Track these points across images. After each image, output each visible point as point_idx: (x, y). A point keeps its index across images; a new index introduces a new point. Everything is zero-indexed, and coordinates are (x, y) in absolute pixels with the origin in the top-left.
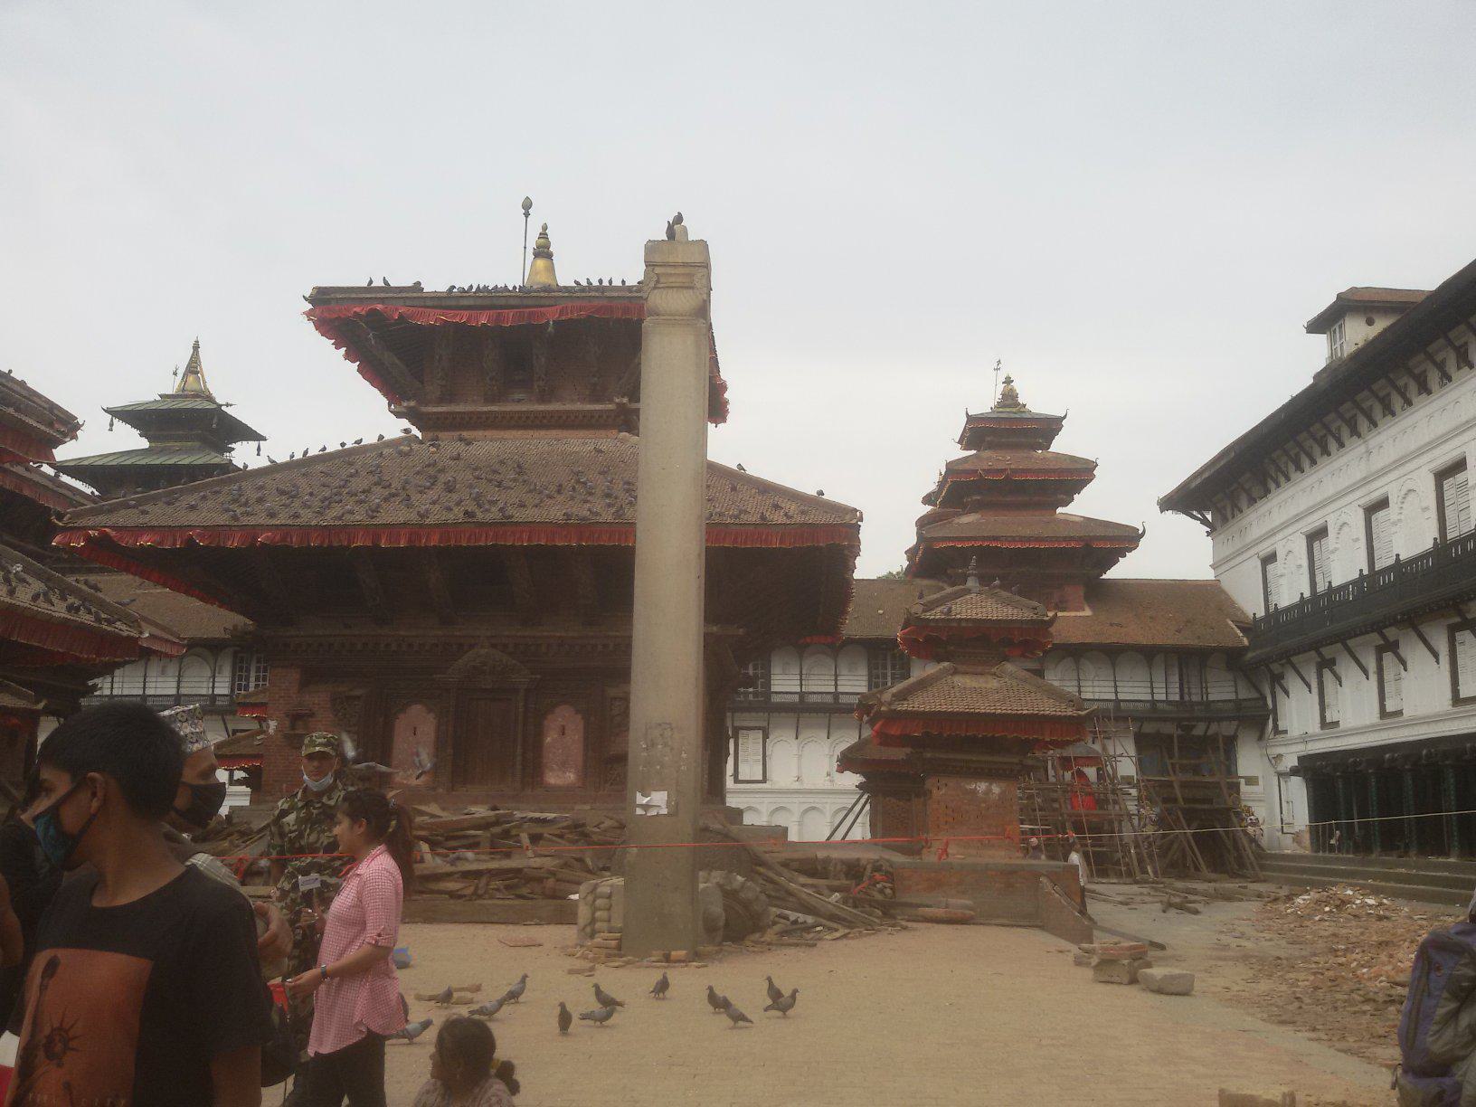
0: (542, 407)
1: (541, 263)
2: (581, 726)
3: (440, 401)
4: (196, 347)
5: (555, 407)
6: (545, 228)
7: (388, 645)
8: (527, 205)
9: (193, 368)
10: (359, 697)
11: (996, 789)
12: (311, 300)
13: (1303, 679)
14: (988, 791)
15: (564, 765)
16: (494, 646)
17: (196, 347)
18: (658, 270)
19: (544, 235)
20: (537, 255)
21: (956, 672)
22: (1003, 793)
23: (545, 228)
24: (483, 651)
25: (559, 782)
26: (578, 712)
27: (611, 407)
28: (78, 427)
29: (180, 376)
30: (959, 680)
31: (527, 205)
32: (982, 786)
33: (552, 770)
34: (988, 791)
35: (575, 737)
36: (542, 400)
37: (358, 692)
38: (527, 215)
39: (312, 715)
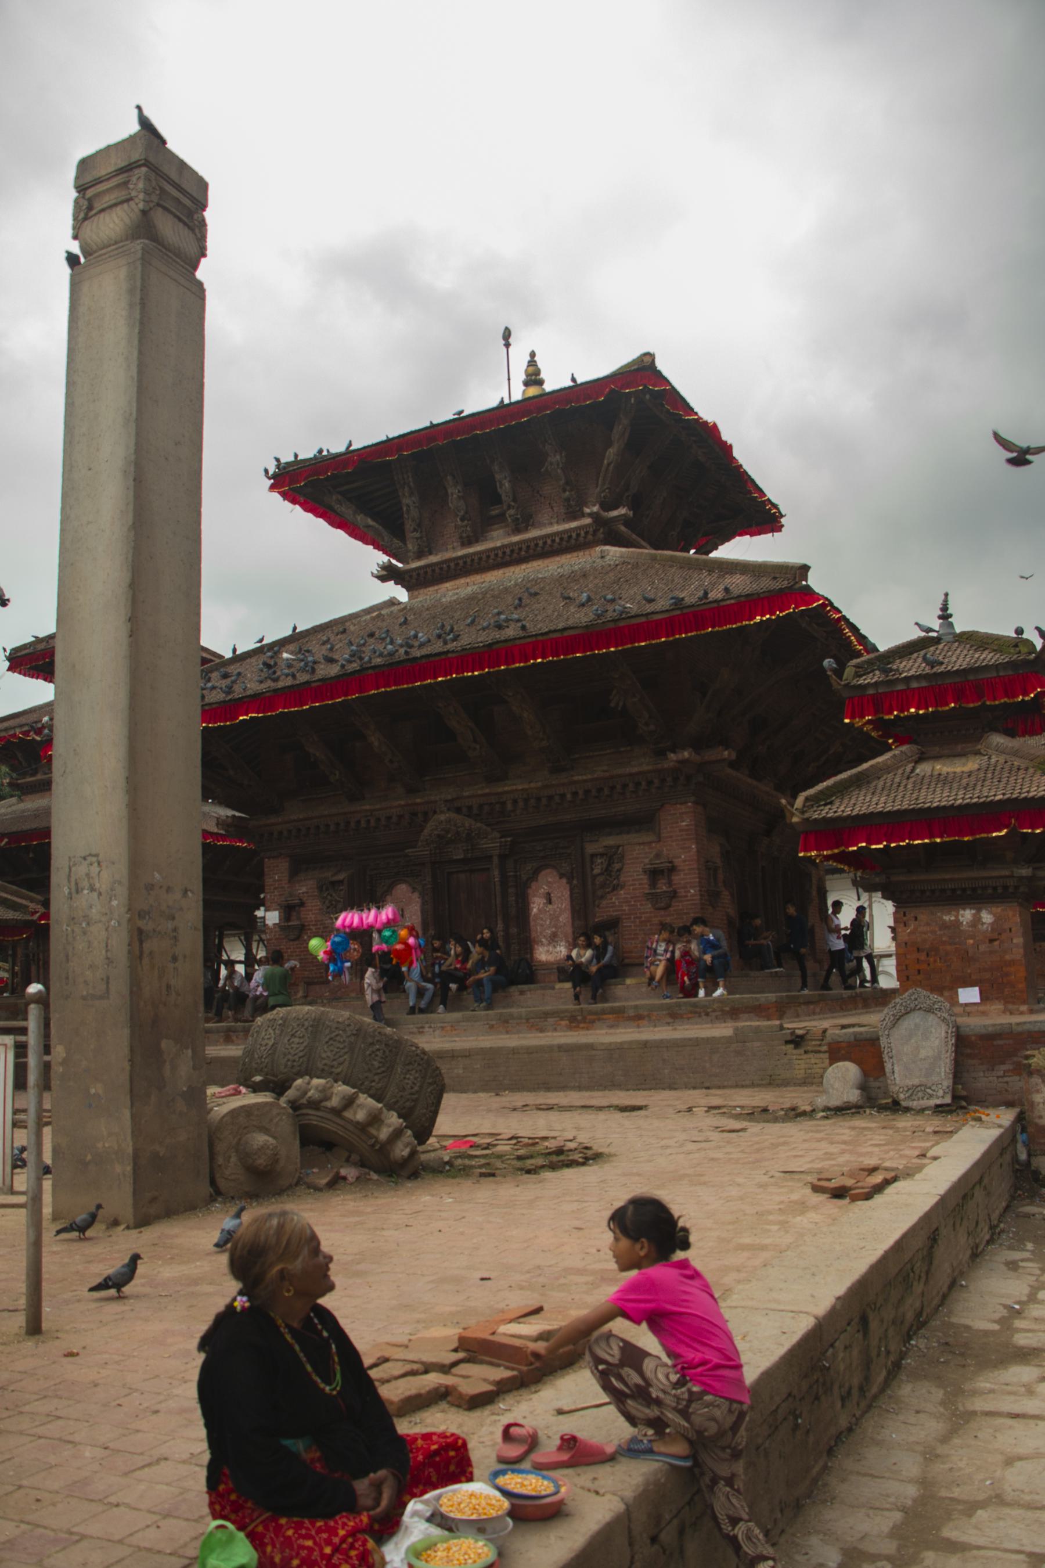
2: (567, 894)
3: (420, 555)
5: (534, 533)
6: (533, 355)
7: (359, 822)
8: (507, 335)
10: (341, 882)
11: (987, 917)
14: (977, 921)
15: (553, 939)
16: (458, 810)
18: (90, 193)
19: (532, 362)
20: (527, 384)
22: (998, 919)
23: (533, 355)
24: (443, 817)
25: (551, 958)
27: (587, 521)
30: (924, 769)
32: (967, 915)
34: (977, 921)
35: (562, 903)
36: (517, 531)
37: (341, 876)
39: (302, 904)
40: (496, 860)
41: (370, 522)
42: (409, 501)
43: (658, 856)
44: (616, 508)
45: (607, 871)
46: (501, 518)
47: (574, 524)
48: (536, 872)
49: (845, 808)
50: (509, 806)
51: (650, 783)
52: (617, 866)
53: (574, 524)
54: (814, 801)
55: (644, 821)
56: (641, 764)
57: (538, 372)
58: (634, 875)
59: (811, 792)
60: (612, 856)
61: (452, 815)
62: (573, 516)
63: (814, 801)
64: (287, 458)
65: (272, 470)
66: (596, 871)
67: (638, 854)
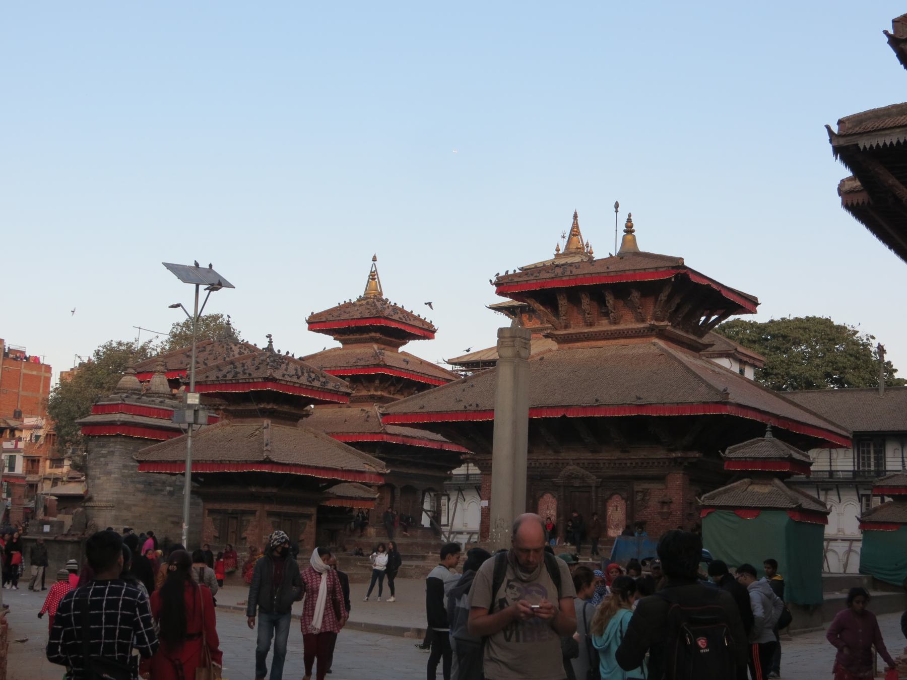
0: (614, 328)
1: (629, 237)
2: (624, 507)
4: (575, 216)
6: (630, 215)
8: (617, 206)
9: (575, 232)
12: (497, 284)
13: (839, 495)
15: (617, 526)
17: (575, 216)
19: (629, 220)
21: (752, 483)
23: (630, 215)
25: (615, 535)
26: (623, 498)
28: (434, 332)
29: (567, 238)
31: (617, 206)
33: (610, 528)
36: (615, 323)
38: (617, 211)
40: (593, 489)
41: (542, 308)
42: (563, 303)
43: (665, 496)
44: (663, 321)
45: (643, 500)
46: (607, 314)
47: (642, 325)
48: (611, 495)
49: (717, 502)
50: (602, 465)
51: (664, 463)
52: (647, 498)
53: (642, 325)
54: (709, 498)
55: (660, 479)
56: (661, 454)
57: (632, 226)
58: (654, 502)
59: (707, 495)
60: (645, 492)
61: (576, 467)
62: (643, 320)
63: (709, 498)
64: (502, 274)
65: (494, 279)
66: (639, 498)
67: (656, 492)
